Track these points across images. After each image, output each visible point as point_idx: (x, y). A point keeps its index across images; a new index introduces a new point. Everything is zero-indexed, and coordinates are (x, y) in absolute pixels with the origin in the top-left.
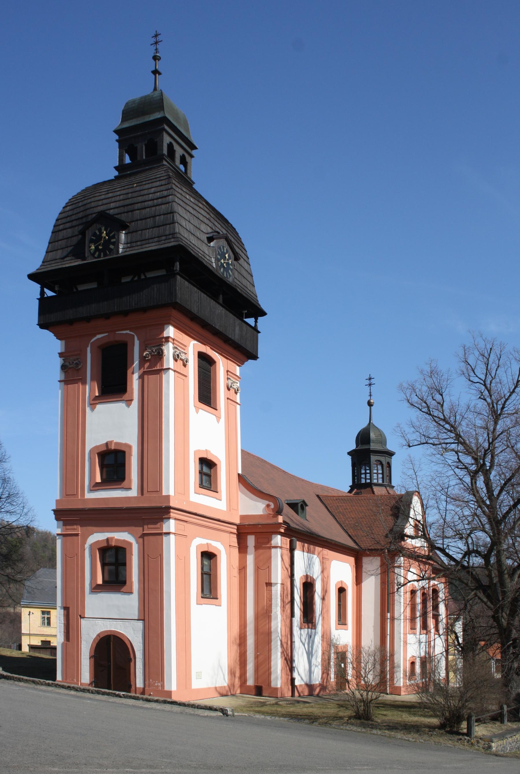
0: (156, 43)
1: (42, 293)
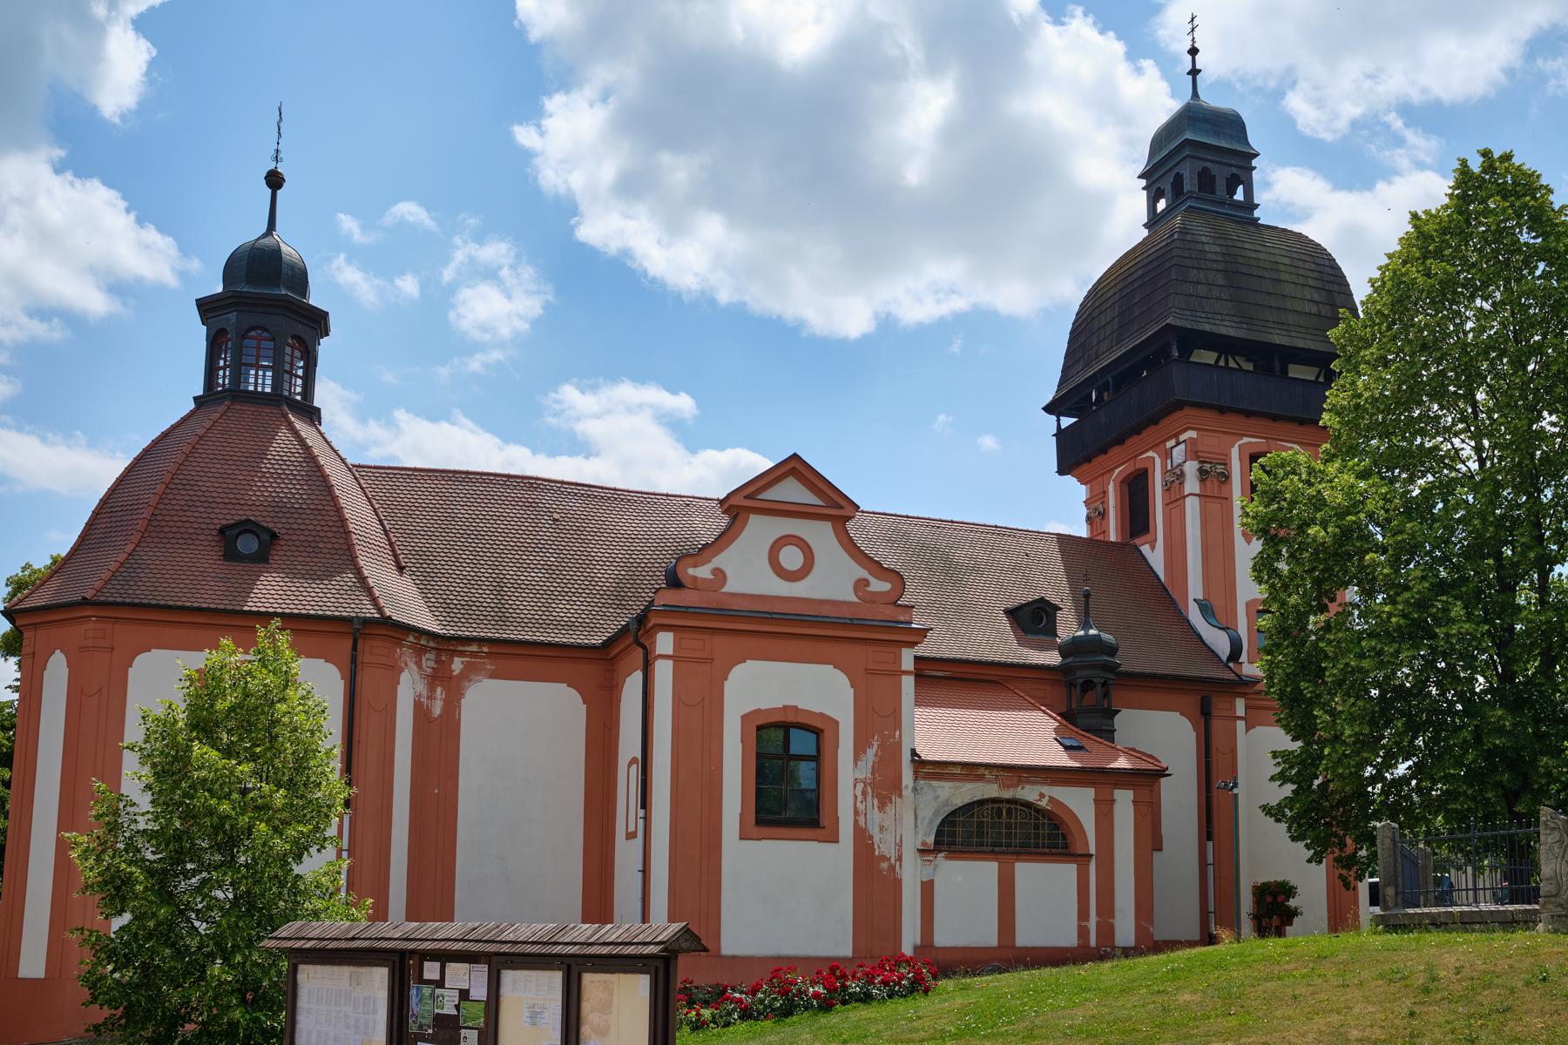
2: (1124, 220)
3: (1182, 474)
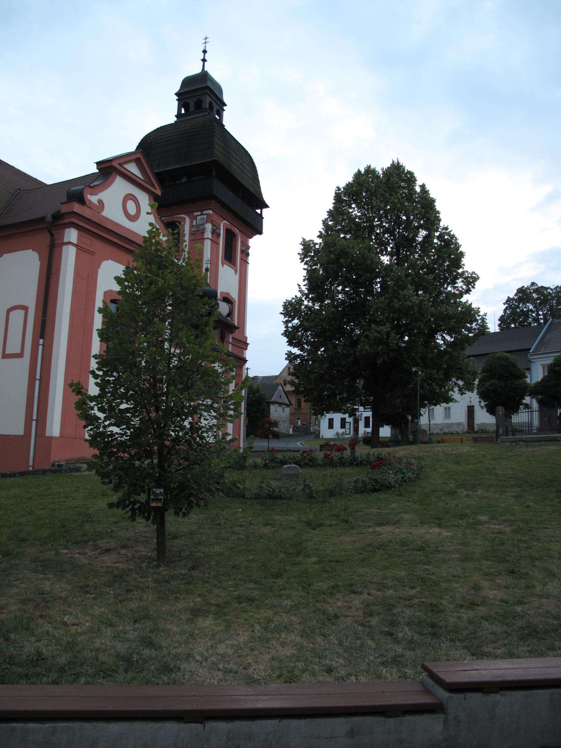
0: (206, 43)
2: (166, 113)
3: (205, 229)
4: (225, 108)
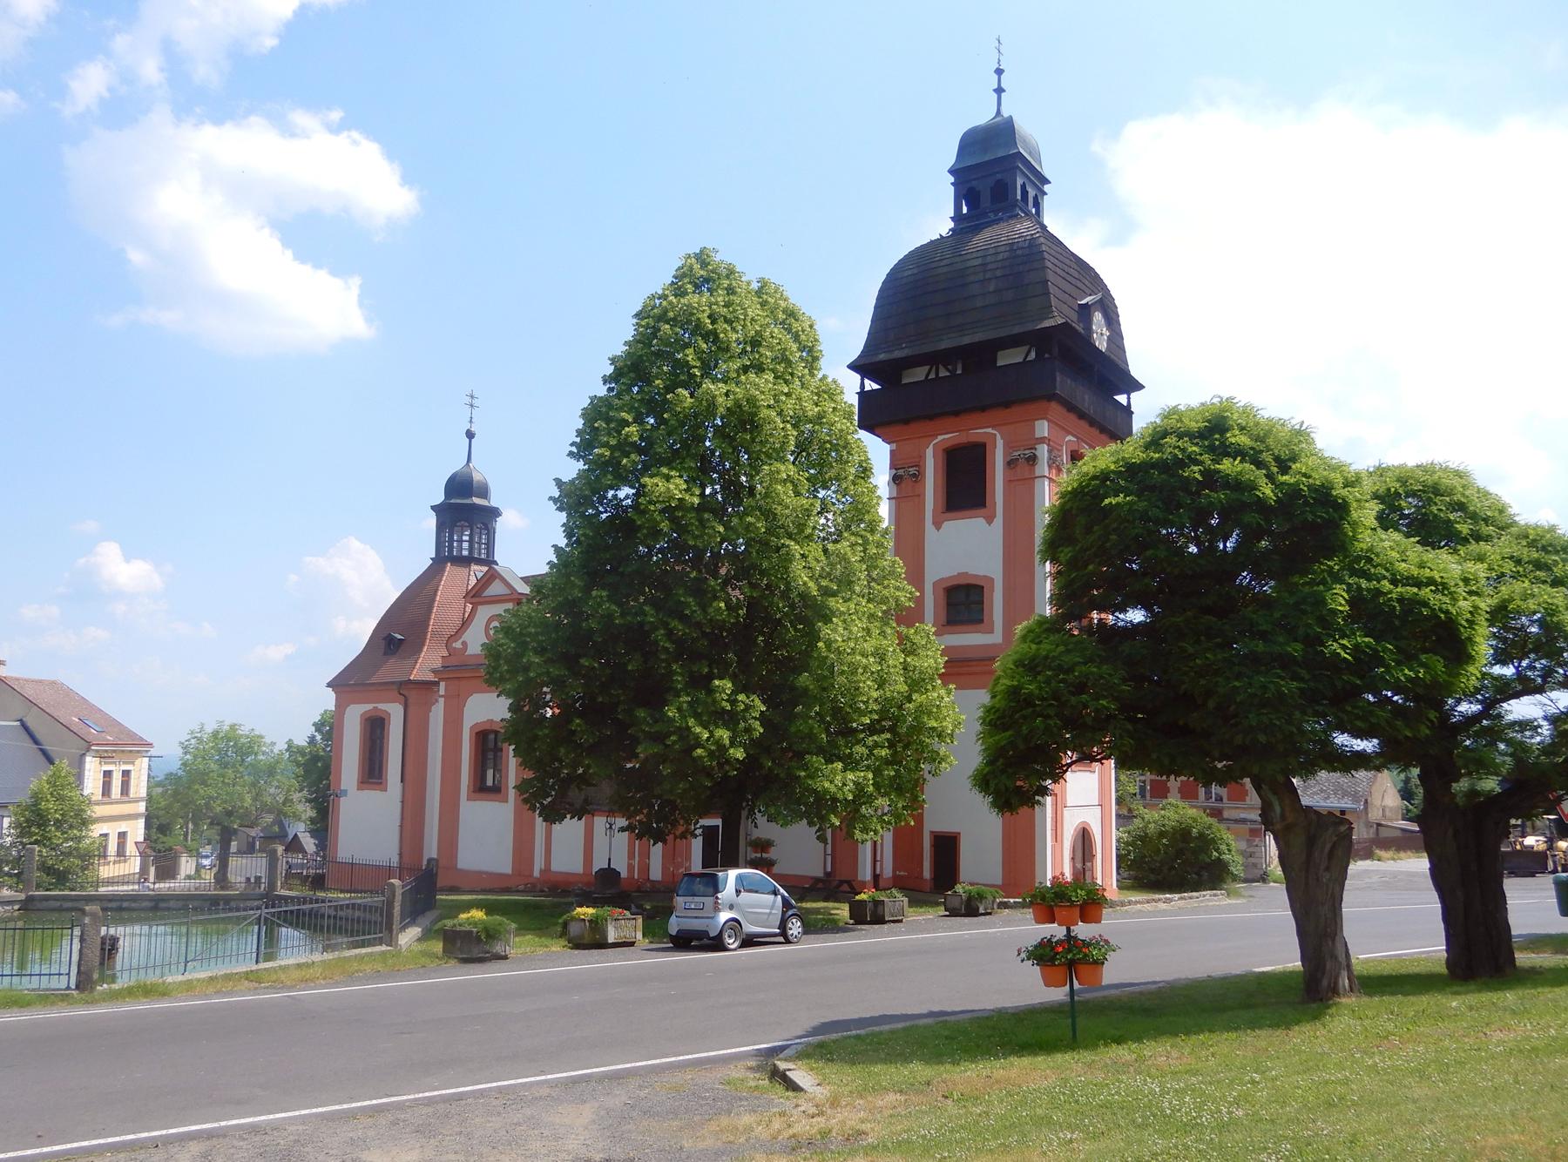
1: (862, 385)
2: (933, 217)
4: (1046, 188)
